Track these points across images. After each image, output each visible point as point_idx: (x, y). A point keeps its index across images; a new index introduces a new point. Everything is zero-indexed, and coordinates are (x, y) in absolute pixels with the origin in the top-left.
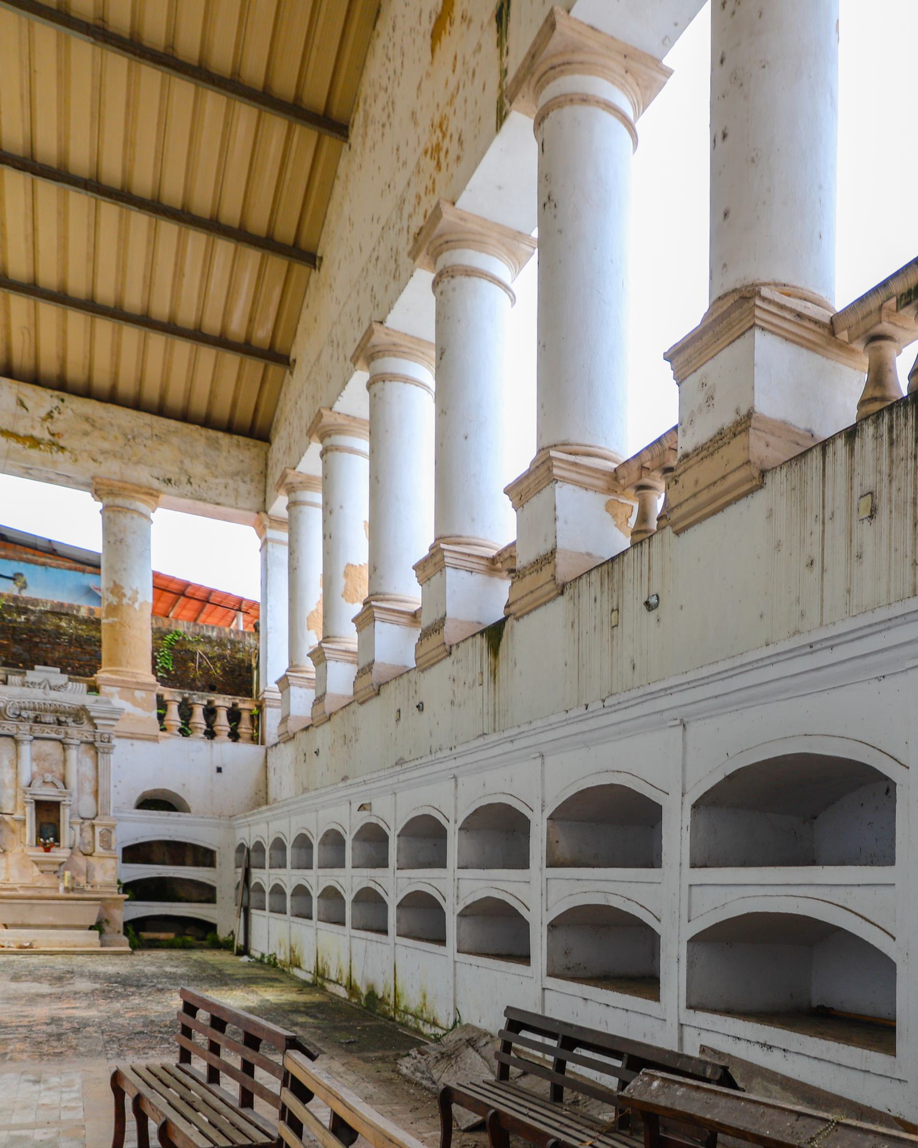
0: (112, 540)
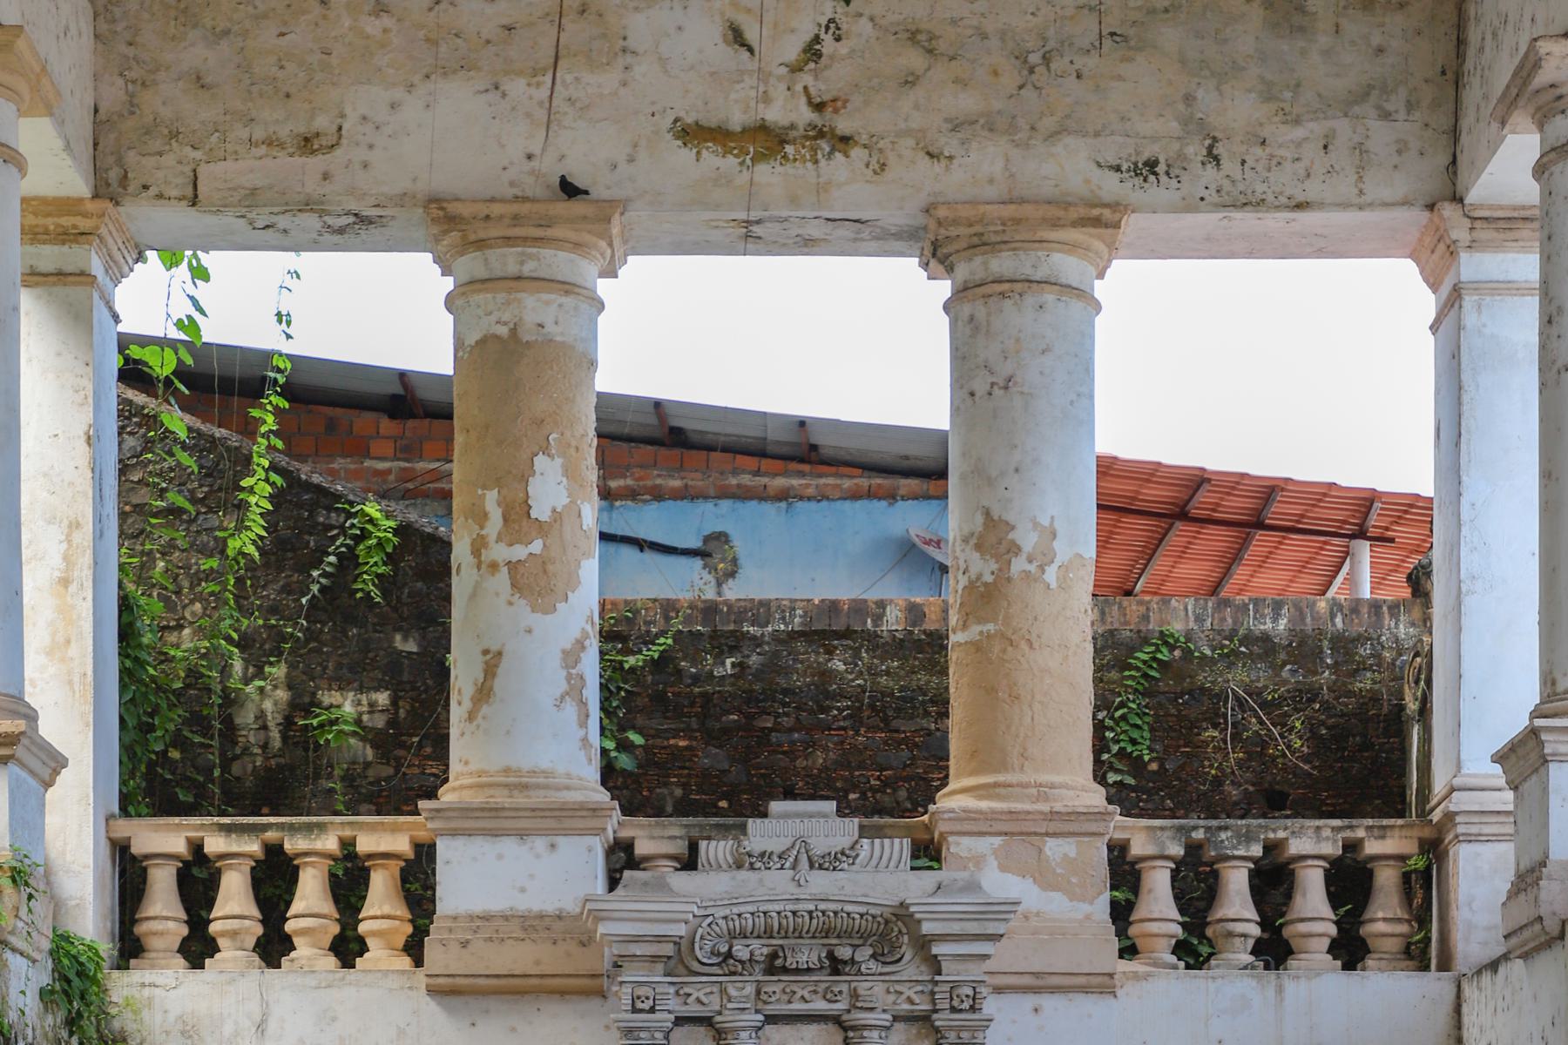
0: (980, 386)
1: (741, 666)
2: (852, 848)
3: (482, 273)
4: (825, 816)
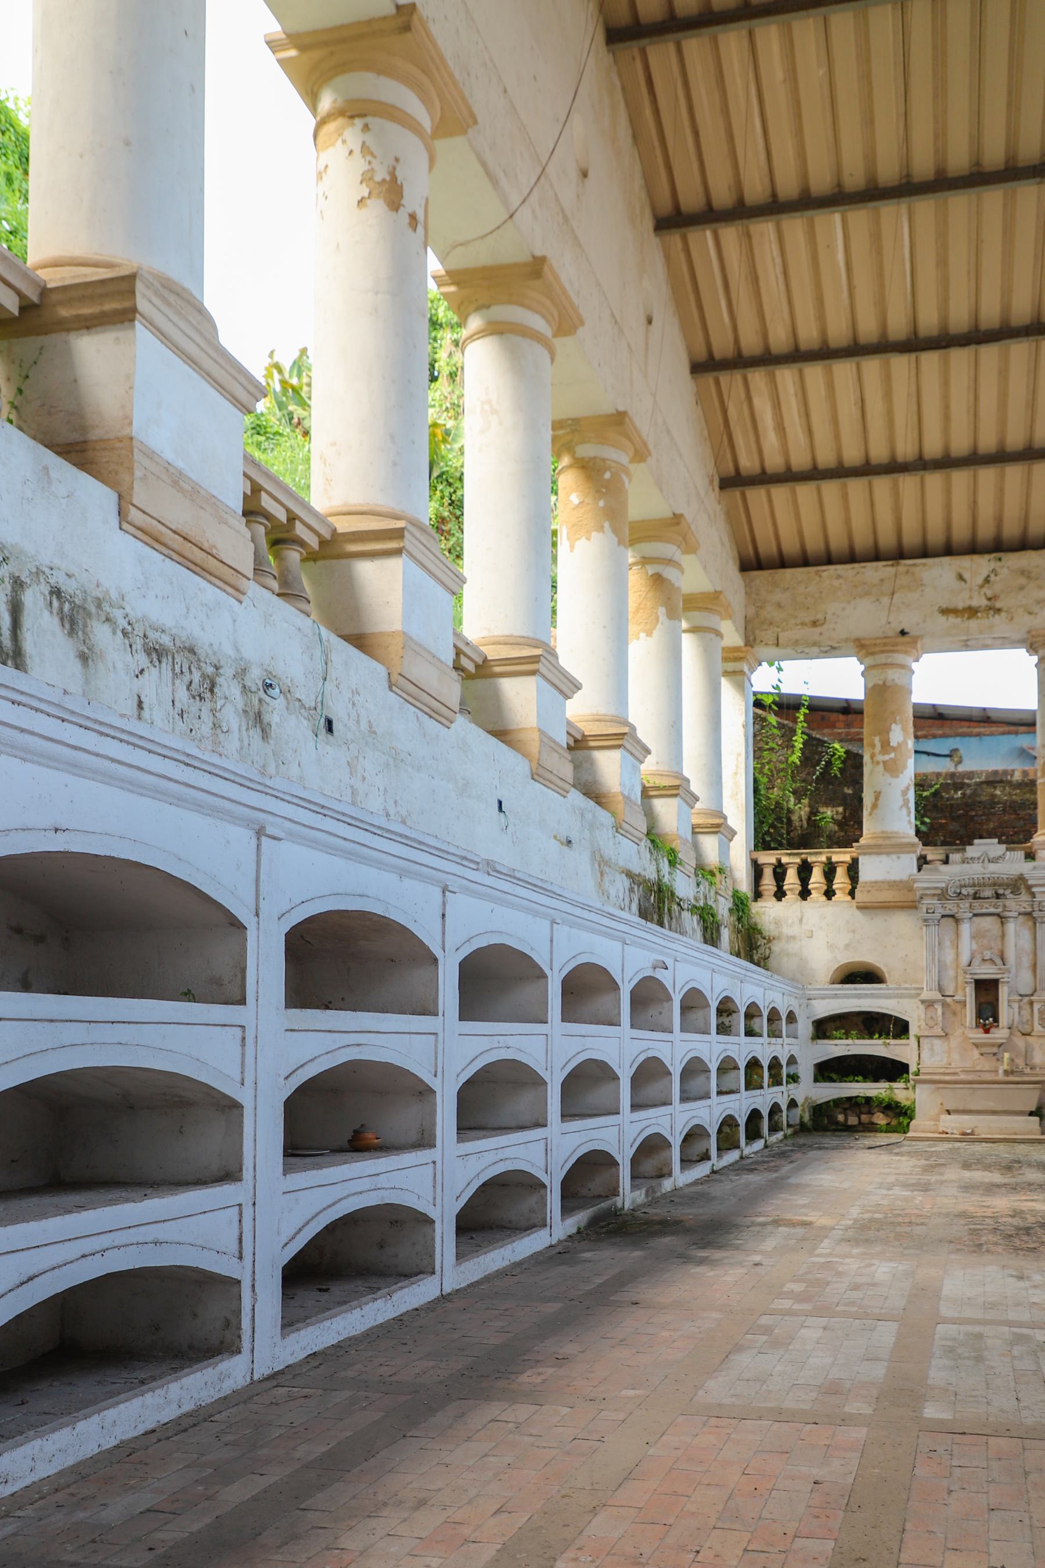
1: (964, 794)
3: (873, 663)
4: (993, 844)
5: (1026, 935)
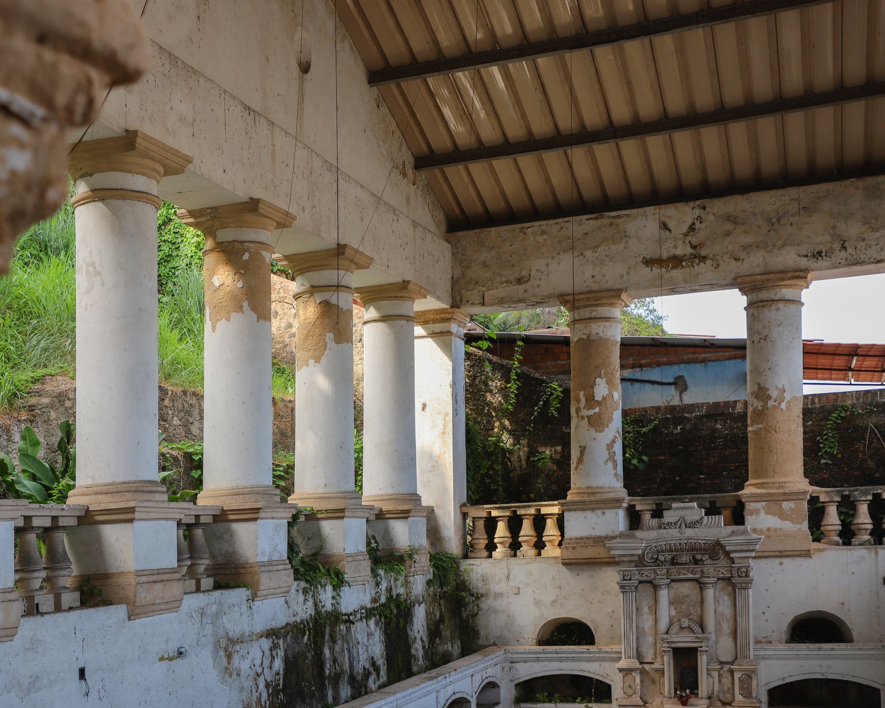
2: (701, 520)
4: (691, 508)
5: (726, 600)
